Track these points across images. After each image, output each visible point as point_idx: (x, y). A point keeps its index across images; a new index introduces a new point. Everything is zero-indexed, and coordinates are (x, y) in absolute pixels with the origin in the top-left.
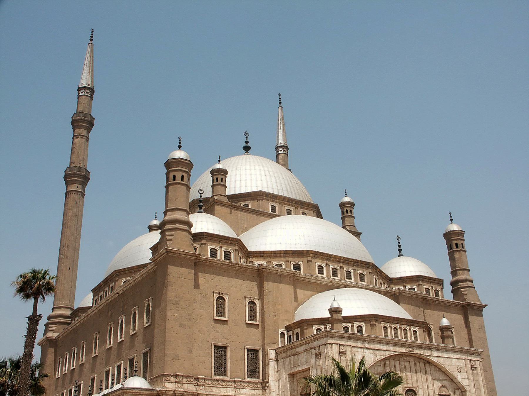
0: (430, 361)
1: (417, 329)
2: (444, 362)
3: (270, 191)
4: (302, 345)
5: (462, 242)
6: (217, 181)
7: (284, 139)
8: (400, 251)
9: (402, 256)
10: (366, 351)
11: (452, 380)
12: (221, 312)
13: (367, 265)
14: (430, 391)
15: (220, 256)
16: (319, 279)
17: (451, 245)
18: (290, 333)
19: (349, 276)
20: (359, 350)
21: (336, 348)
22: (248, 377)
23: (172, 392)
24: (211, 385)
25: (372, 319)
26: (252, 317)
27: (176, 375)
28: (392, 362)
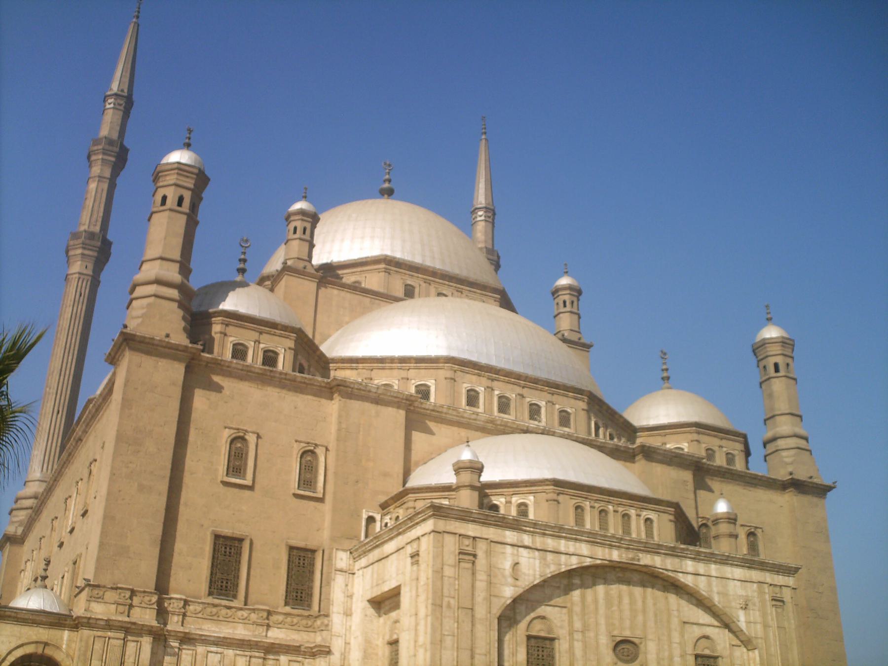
0: (677, 583)
1: (652, 515)
2: (709, 584)
5: (789, 360)
6: (295, 232)
7: (486, 195)
11: (727, 625)
13: (578, 391)
15: (254, 358)
16: (466, 415)
17: (765, 367)
18: (387, 519)
19: (534, 412)
20: (509, 549)
22: (286, 604)
24: (200, 615)
27: (117, 588)
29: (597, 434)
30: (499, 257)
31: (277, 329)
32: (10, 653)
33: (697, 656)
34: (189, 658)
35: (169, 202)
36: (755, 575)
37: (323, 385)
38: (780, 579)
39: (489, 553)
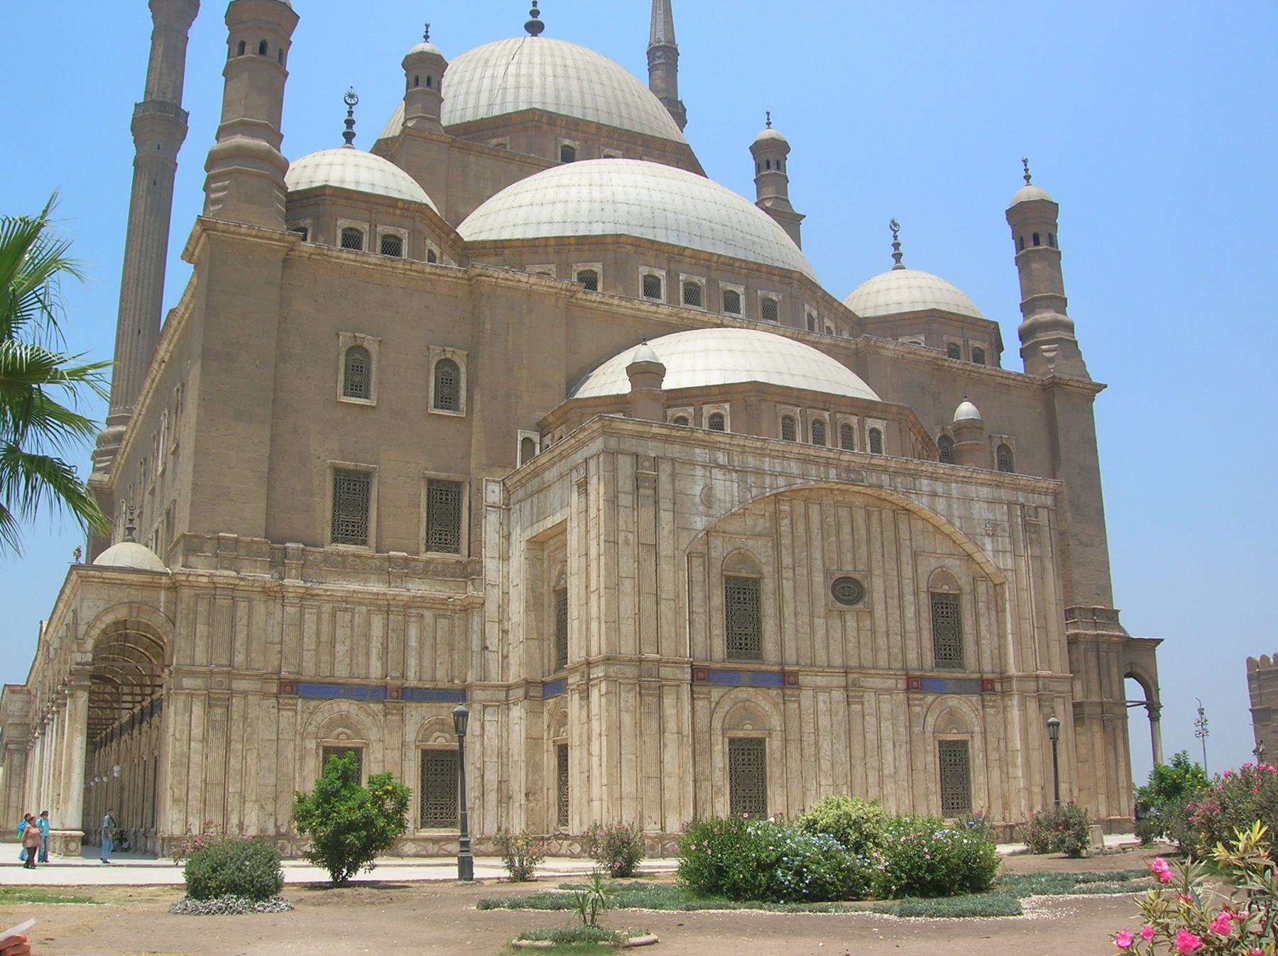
1: (879, 425)
2: (949, 507)
3: (564, 111)
4: (554, 464)
8: (897, 257)
9: (903, 268)
10: (718, 473)
12: (357, 381)
14: (906, 582)
16: (643, 307)
18: (547, 440)
20: (699, 472)
21: (625, 464)
23: (205, 580)
25: (751, 400)
26: (446, 398)
27: (219, 538)
28: (800, 507)
29: (811, 327)
30: (685, 110)
31: (396, 207)
32: (98, 618)
33: (933, 595)
34: (314, 618)
35: (248, 48)
36: (1004, 494)
37: (460, 275)
38: (1036, 499)
39: (673, 476)
